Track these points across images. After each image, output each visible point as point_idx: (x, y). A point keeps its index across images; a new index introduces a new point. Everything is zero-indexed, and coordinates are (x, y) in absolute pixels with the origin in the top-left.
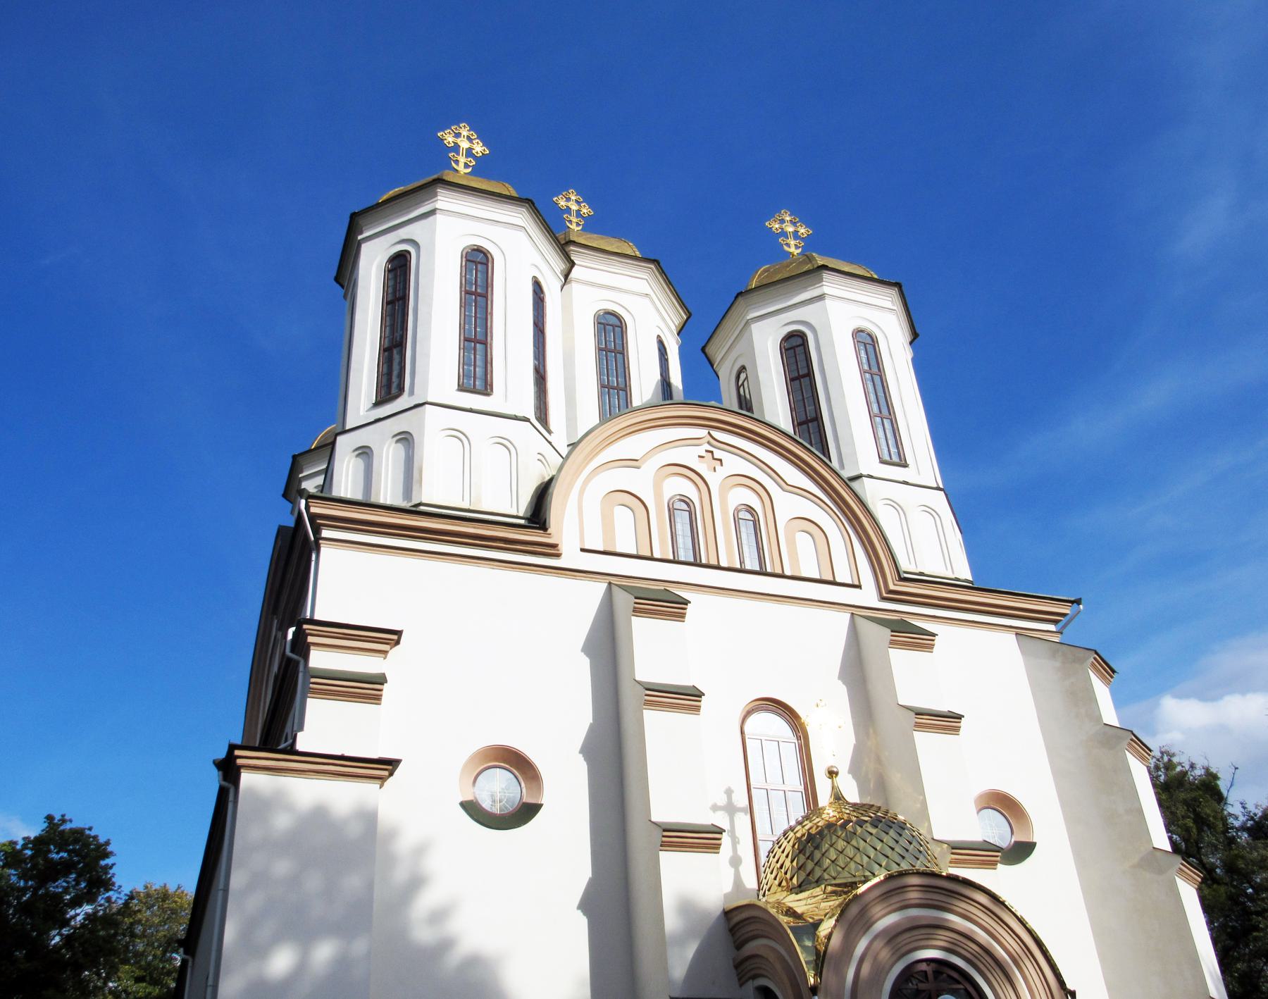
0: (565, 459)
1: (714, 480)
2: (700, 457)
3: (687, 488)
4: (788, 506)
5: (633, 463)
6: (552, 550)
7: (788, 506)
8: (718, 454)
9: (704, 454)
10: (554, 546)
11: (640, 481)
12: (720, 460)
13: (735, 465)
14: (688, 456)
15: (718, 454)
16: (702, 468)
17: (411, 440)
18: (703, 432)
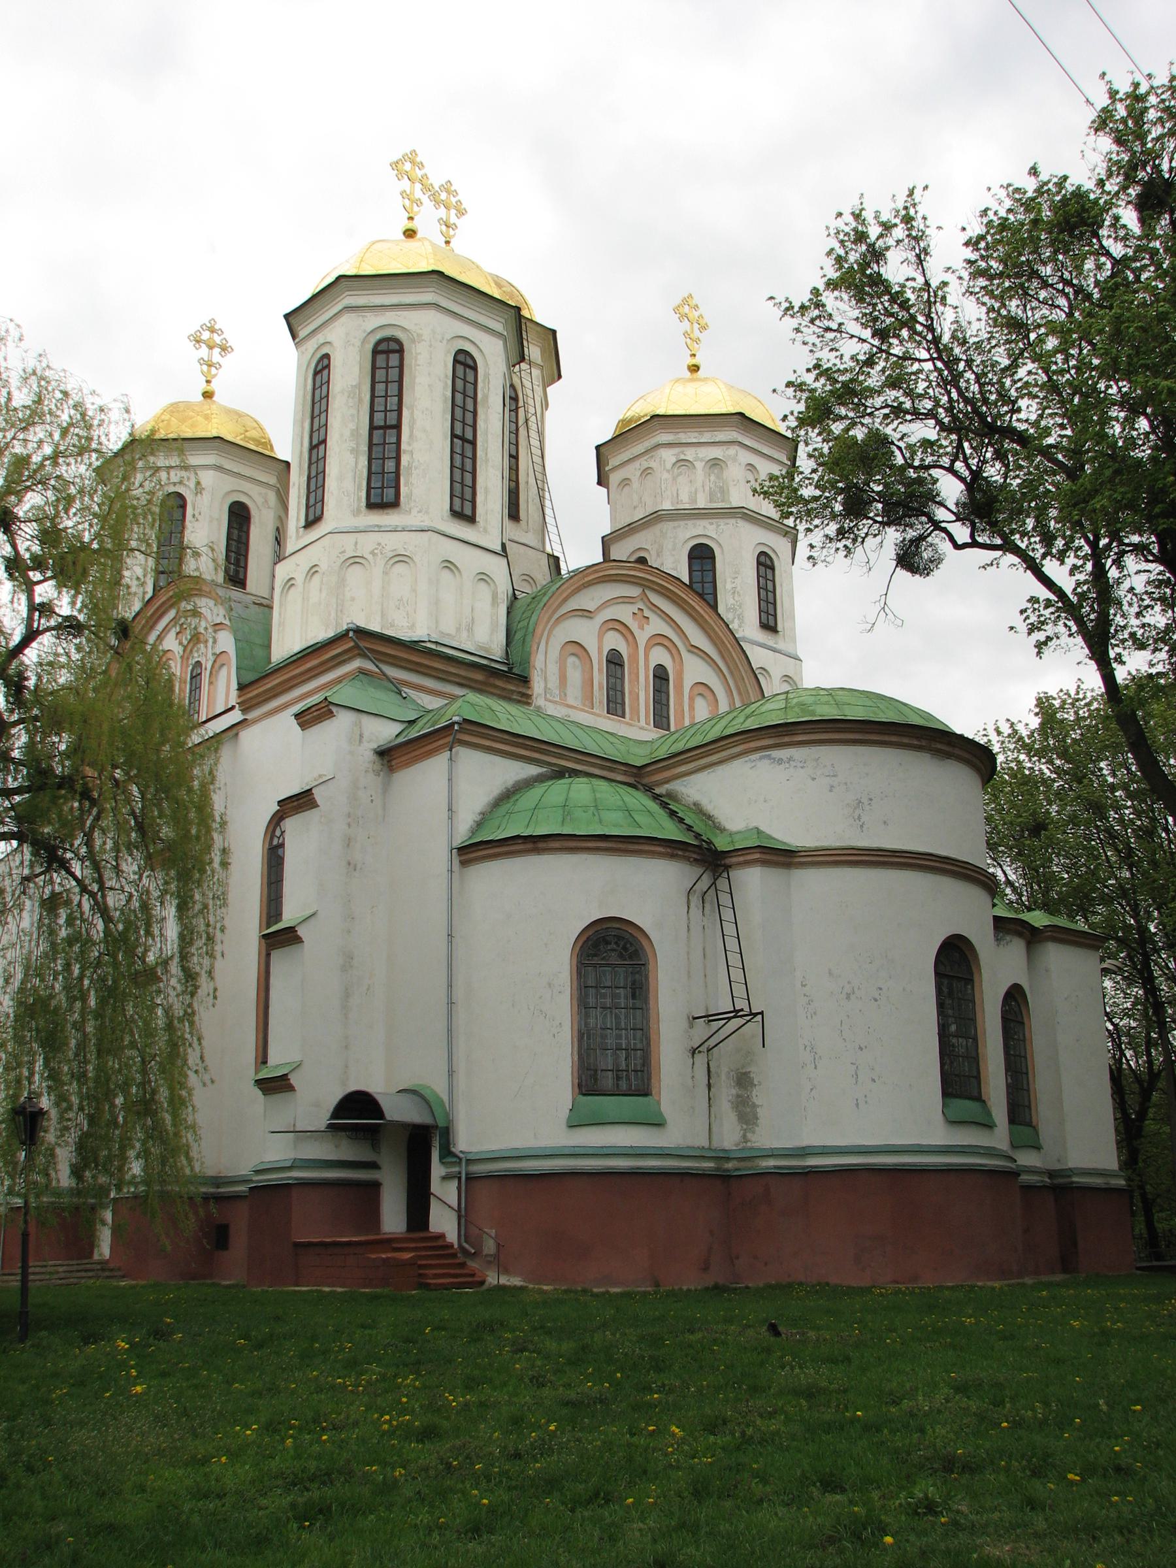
0: (514, 589)
1: (642, 637)
3: (623, 649)
4: (694, 671)
5: (586, 614)
6: (529, 696)
7: (694, 671)
8: (647, 613)
9: (636, 612)
11: (584, 632)
13: (657, 626)
14: (624, 613)
15: (647, 613)
16: (634, 626)
17: (412, 565)
18: (635, 591)
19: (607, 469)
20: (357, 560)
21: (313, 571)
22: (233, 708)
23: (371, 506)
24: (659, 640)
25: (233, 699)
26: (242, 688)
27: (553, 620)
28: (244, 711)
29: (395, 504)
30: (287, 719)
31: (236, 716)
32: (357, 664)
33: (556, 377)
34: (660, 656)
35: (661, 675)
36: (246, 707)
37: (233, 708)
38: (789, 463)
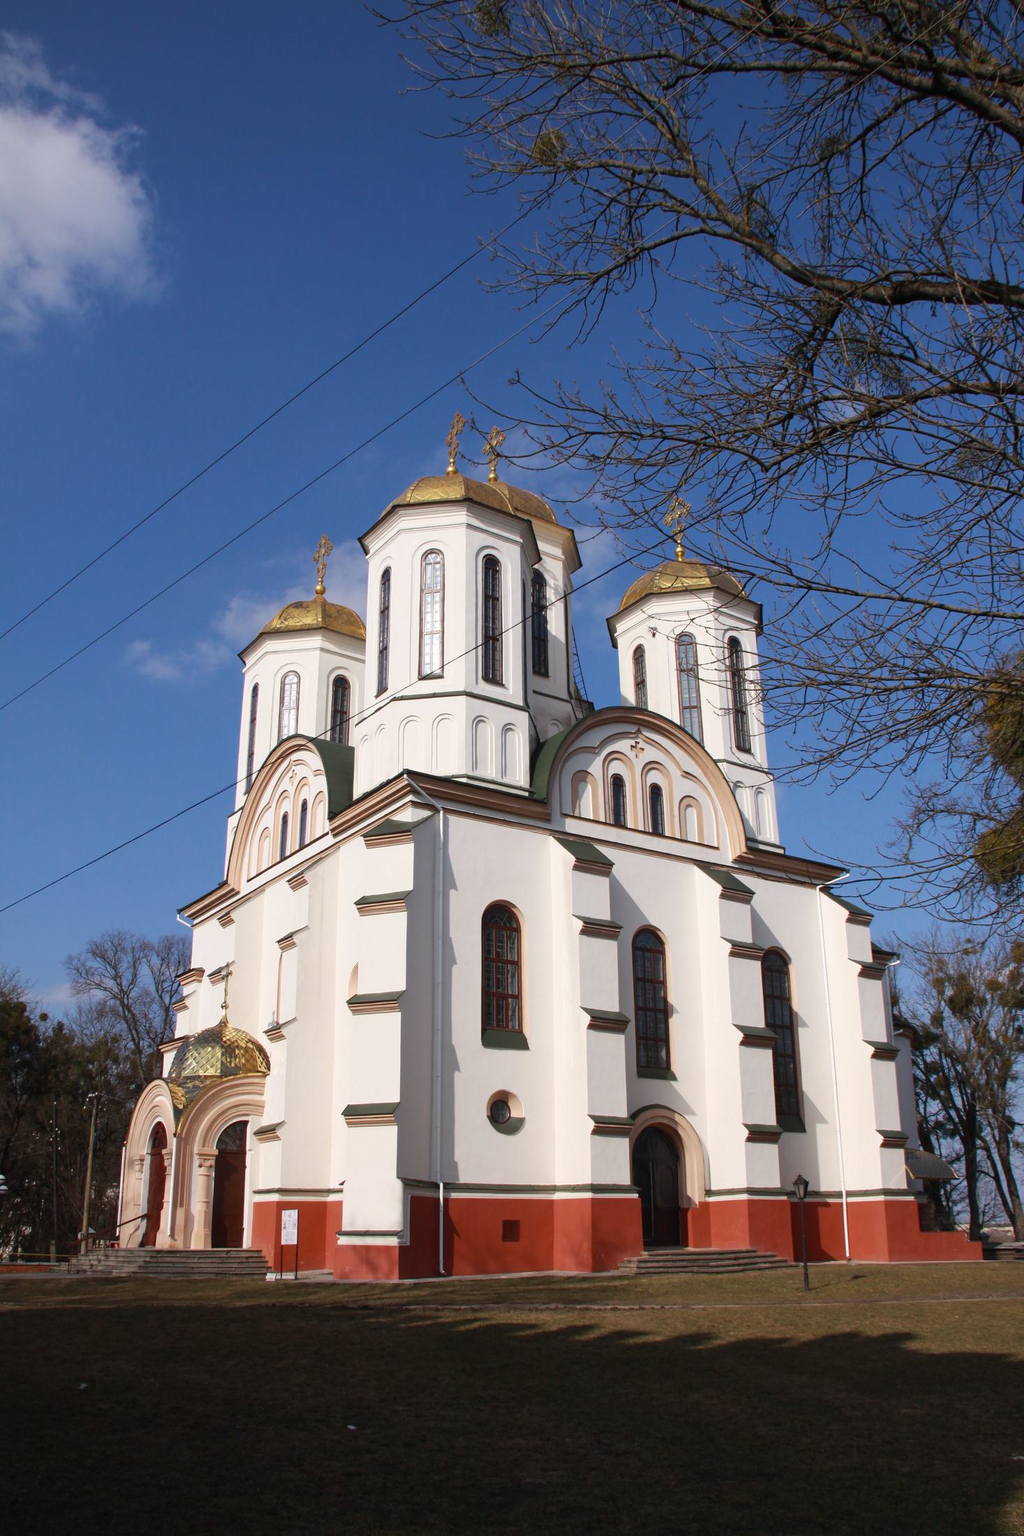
2: (632, 746)
10: (549, 815)
12: (643, 749)
15: (642, 744)
16: (631, 754)
19: (616, 635)
20: (410, 719)
21: (381, 727)
22: (327, 834)
23: (423, 678)
24: (651, 766)
25: (327, 826)
26: (332, 816)
27: (566, 755)
28: (335, 836)
29: (441, 677)
30: (359, 841)
31: (330, 840)
32: (411, 797)
33: (578, 565)
34: (654, 777)
35: (656, 791)
36: (336, 832)
37: (327, 834)
38: (756, 622)
